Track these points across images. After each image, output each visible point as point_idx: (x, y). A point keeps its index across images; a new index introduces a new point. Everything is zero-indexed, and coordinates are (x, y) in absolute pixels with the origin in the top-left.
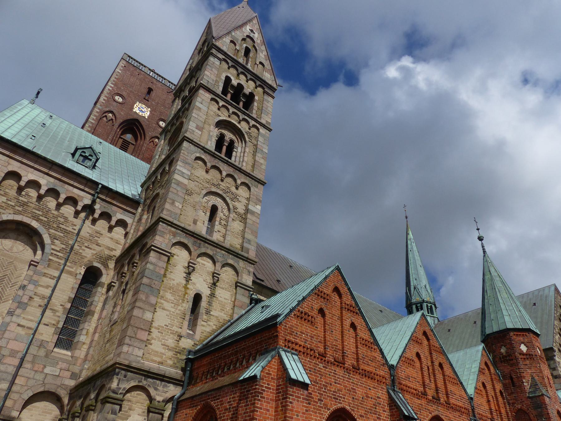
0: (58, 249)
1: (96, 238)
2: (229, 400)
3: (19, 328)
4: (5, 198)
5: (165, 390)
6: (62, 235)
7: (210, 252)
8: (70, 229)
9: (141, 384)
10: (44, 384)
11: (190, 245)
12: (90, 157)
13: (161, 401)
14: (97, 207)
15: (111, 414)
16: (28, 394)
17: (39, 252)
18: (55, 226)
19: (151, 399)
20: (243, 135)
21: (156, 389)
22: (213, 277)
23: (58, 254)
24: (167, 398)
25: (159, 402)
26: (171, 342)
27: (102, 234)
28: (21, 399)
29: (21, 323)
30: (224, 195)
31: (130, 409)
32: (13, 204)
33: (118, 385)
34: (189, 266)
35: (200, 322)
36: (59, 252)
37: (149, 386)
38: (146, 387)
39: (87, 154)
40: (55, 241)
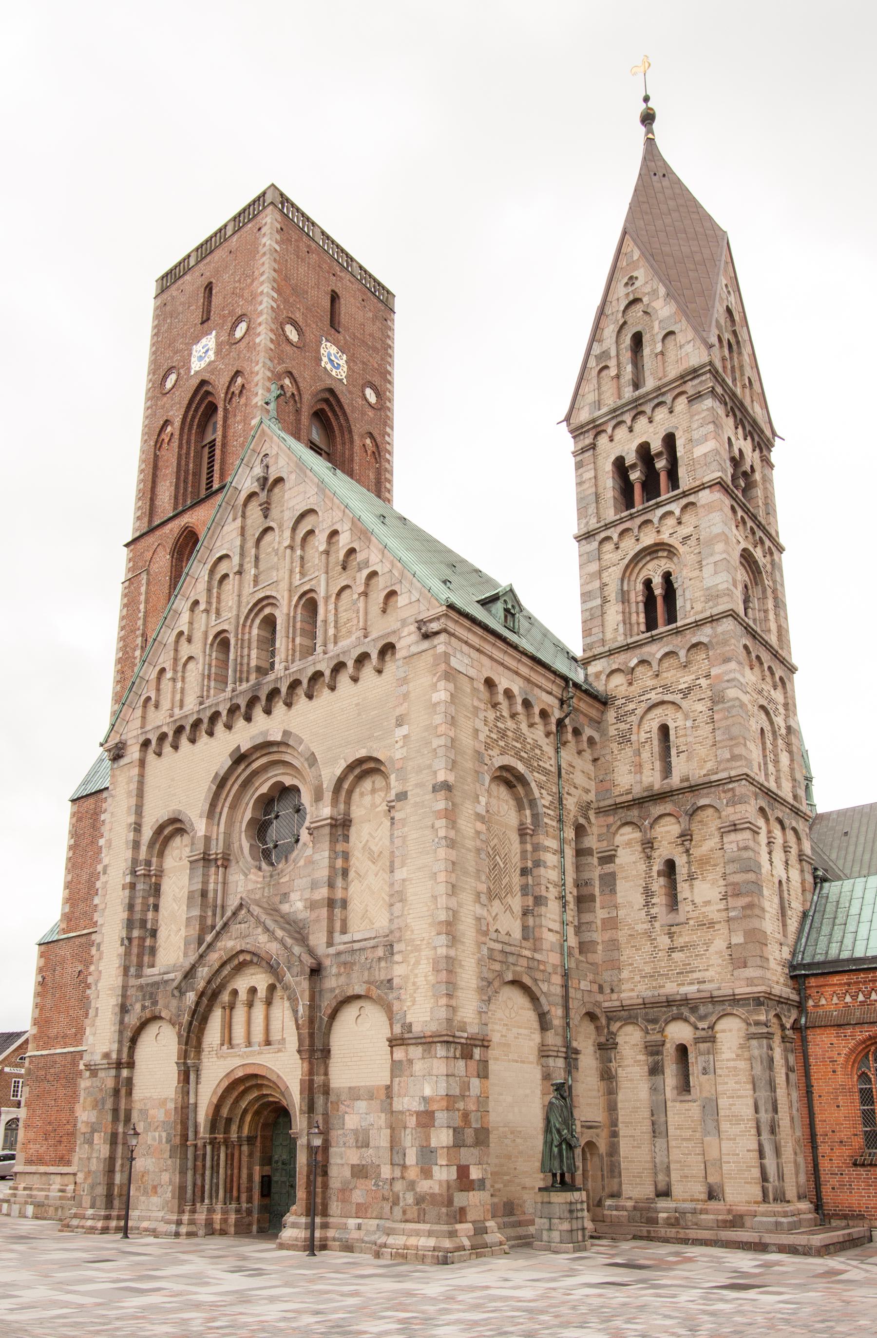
0: (547, 804)
1: (571, 776)
3: (551, 934)
4: (487, 728)
6: (544, 778)
7: (780, 815)
8: (547, 766)
11: (767, 809)
12: (512, 611)
14: (567, 721)
17: (528, 812)
18: (536, 765)
20: (760, 573)
22: (785, 852)
23: (550, 812)
26: (777, 954)
27: (574, 767)
29: (550, 927)
30: (769, 707)
32: (494, 736)
34: (769, 843)
35: (789, 922)
36: (549, 808)
39: (509, 606)
40: (543, 791)
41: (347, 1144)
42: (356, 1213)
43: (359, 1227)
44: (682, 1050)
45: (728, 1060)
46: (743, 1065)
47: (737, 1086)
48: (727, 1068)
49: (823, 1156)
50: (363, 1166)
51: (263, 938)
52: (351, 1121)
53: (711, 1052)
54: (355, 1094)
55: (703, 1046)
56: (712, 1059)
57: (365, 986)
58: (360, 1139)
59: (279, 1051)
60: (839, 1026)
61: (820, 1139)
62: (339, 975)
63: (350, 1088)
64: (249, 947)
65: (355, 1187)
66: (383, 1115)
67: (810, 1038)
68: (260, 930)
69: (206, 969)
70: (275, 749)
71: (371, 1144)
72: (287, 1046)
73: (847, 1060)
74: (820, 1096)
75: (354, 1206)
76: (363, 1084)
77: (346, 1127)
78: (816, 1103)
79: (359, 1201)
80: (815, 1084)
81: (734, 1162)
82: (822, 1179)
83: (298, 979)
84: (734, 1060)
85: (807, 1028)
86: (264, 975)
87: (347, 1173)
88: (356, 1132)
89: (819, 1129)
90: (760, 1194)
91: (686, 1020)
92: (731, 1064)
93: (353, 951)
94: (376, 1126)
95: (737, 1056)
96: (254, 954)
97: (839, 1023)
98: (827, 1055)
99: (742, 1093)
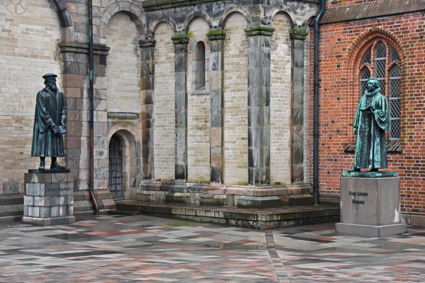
2: (418, 28)
5: (303, 12)
9: (282, 10)
10: (117, 3)
13: (301, 25)
15: (266, 46)
16: (106, 17)
19: (292, 24)
21: (295, 13)
24: (305, 21)
25: (299, 26)
28: (102, 24)
31: (276, 39)
33: (265, 15)
37: (289, 10)
38: (287, 12)
44: (201, 45)
45: (233, 56)
46: (243, 61)
47: (239, 81)
48: (232, 64)
49: (323, 144)
53: (222, 49)
55: (214, 43)
56: (220, 55)
60: (347, 21)
61: (322, 129)
67: (323, 34)
73: (350, 55)
74: (325, 90)
78: (322, 96)
80: (323, 79)
81: (232, 149)
82: (321, 165)
84: (238, 56)
85: (320, 25)
89: (322, 119)
90: (247, 177)
91: (204, 18)
92: (235, 60)
95: (241, 52)
97: (347, 19)
98: (335, 50)
99: (239, 87)
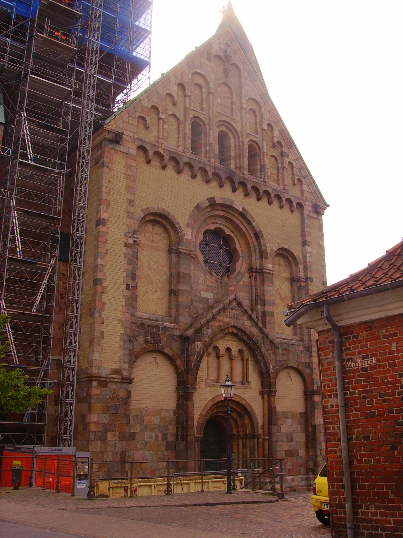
41: (283, 441)
42: (288, 474)
43: (293, 480)
50: (291, 450)
51: (248, 324)
52: (284, 429)
54: (286, 415)
57: (296, 364)
58: (289, 438)
59: (247, 388)
62: (283, 355)
63: (283, 412)
64: (239, 326)
65: (287, 461)
66: (299, 426)
68: (245, 318)
69: (210, 331)
70: (231, 212)
71: (294, 440)
72: (251, 386)
75: (287, 470)
76: (289, 411)
77: (282, 432)
79: (289, 468)
83: (269, 352)
86: (236, 343)
87: (283, 454)
88: (287, 434)
93: (288, 344)
94: (296, 431)
96: (239, 329)
